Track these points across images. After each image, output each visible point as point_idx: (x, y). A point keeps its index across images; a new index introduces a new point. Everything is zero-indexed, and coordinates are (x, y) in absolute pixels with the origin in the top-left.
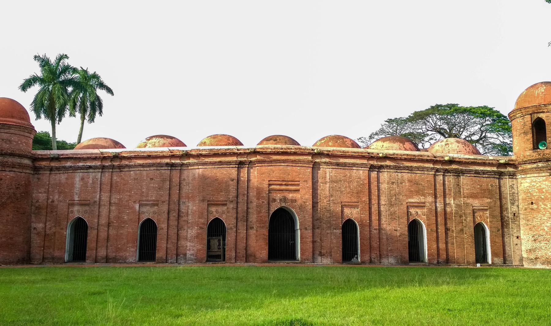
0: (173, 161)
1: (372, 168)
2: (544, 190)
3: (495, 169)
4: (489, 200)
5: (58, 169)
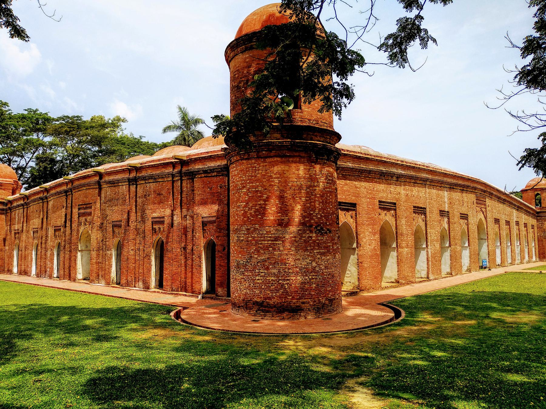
3: (224, 162)
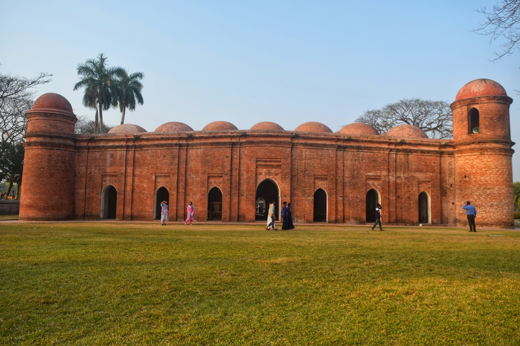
0: (181, 142)
1: (339, 147)
2: (475, 166)
3: (437, 149)
4: (431, 174)
5: (94, 148)
